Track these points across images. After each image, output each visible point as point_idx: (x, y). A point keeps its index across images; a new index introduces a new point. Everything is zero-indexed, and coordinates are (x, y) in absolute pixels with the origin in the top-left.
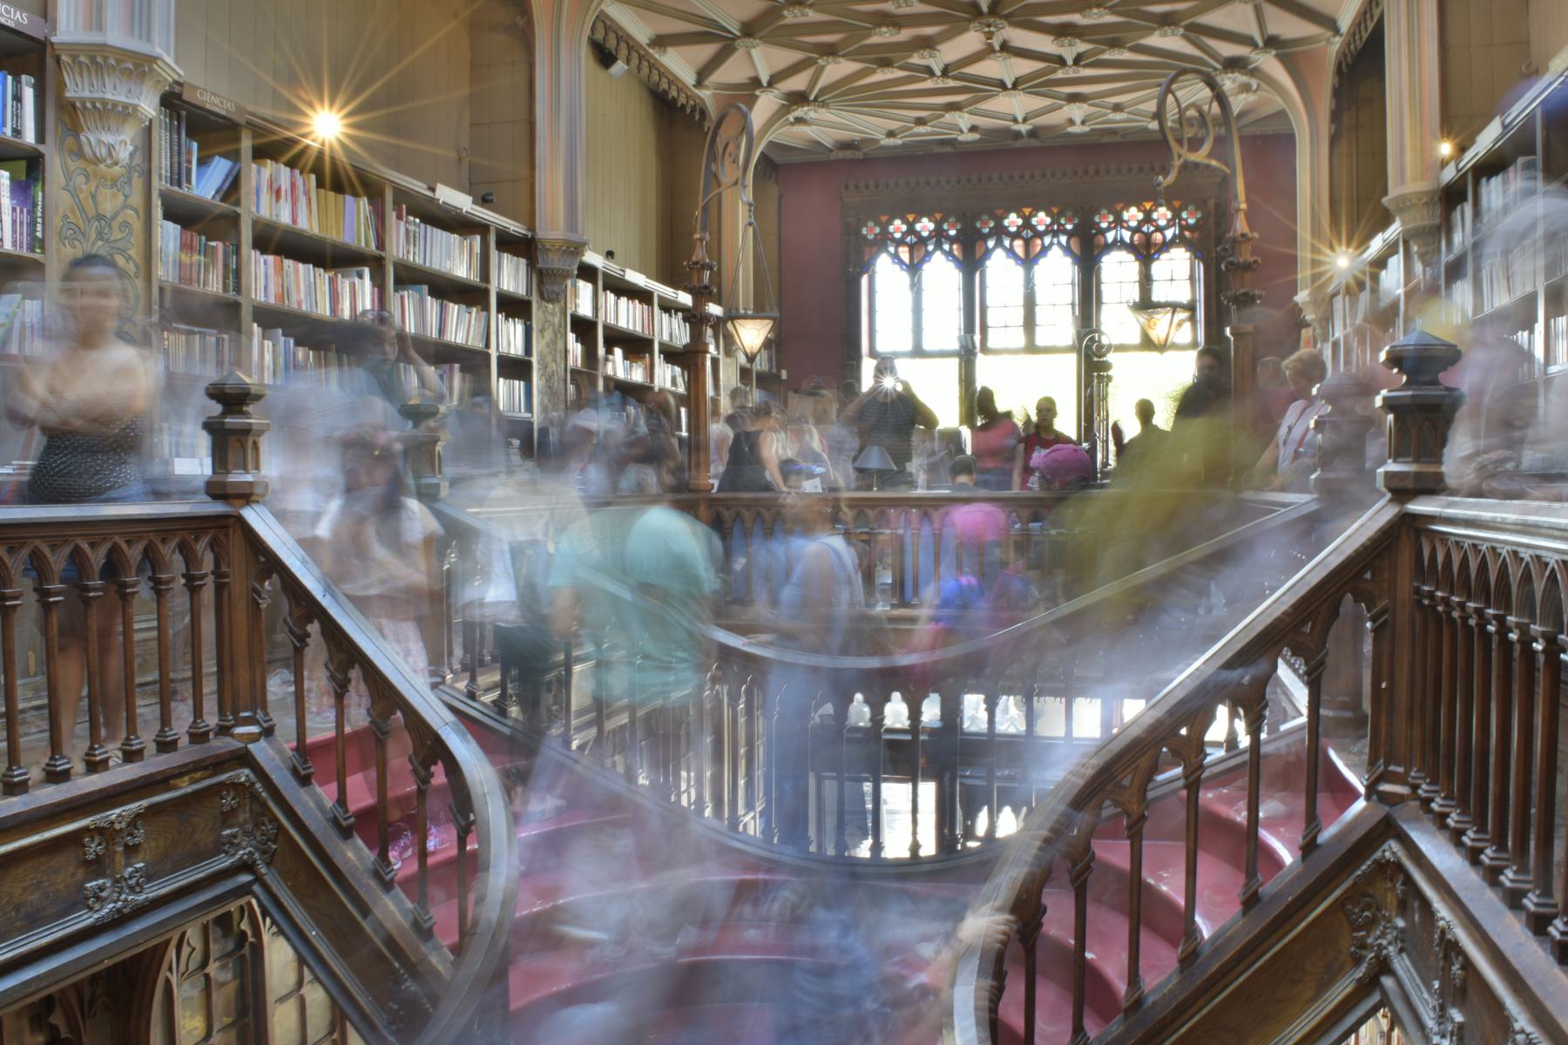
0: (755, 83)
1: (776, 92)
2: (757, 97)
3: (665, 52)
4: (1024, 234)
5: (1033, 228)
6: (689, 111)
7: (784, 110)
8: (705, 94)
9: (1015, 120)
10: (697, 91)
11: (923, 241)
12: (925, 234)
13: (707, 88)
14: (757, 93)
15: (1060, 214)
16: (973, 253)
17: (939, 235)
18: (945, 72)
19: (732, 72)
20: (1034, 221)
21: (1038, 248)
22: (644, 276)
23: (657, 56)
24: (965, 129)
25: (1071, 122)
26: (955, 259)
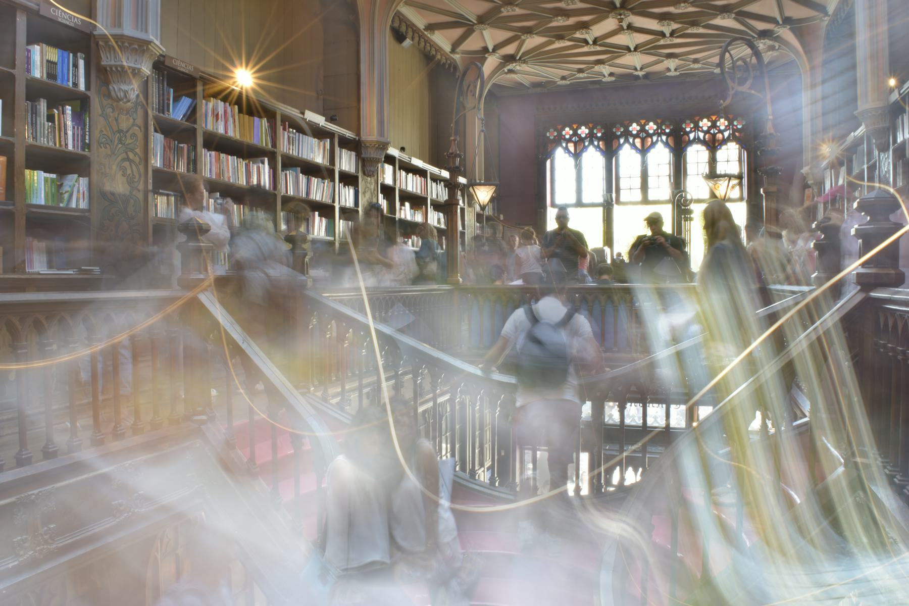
0: (485, 50)
1: (497, 55)
2: (486, 58)
3: (434, 33)
4: (641, 135)
5: (646, 132)
6: (447, 66)
7: (501, 66)
8: (457, 57)
9: (636, 69)
10: (452, 55)
11: (582, 140)
12: (583, 136)
13: (458, 53)
14: (486, 56)
15: (663, 123)
16: (612, 146)
17: (591, 136)
18: (595, 42)
19: (472, 44)
20: (647, 128)
21: (649, 143)
22: (422, 162)
23: (429, 35)
24: (606, 75)
25: (668, 70)
26: (601, 150)
